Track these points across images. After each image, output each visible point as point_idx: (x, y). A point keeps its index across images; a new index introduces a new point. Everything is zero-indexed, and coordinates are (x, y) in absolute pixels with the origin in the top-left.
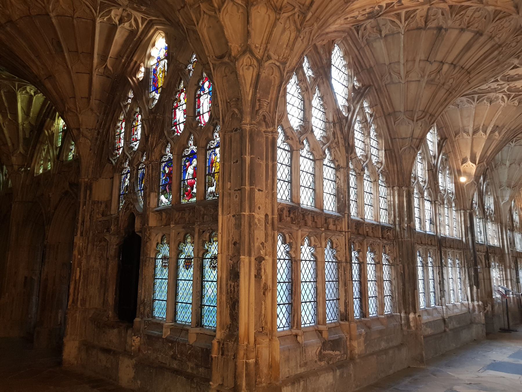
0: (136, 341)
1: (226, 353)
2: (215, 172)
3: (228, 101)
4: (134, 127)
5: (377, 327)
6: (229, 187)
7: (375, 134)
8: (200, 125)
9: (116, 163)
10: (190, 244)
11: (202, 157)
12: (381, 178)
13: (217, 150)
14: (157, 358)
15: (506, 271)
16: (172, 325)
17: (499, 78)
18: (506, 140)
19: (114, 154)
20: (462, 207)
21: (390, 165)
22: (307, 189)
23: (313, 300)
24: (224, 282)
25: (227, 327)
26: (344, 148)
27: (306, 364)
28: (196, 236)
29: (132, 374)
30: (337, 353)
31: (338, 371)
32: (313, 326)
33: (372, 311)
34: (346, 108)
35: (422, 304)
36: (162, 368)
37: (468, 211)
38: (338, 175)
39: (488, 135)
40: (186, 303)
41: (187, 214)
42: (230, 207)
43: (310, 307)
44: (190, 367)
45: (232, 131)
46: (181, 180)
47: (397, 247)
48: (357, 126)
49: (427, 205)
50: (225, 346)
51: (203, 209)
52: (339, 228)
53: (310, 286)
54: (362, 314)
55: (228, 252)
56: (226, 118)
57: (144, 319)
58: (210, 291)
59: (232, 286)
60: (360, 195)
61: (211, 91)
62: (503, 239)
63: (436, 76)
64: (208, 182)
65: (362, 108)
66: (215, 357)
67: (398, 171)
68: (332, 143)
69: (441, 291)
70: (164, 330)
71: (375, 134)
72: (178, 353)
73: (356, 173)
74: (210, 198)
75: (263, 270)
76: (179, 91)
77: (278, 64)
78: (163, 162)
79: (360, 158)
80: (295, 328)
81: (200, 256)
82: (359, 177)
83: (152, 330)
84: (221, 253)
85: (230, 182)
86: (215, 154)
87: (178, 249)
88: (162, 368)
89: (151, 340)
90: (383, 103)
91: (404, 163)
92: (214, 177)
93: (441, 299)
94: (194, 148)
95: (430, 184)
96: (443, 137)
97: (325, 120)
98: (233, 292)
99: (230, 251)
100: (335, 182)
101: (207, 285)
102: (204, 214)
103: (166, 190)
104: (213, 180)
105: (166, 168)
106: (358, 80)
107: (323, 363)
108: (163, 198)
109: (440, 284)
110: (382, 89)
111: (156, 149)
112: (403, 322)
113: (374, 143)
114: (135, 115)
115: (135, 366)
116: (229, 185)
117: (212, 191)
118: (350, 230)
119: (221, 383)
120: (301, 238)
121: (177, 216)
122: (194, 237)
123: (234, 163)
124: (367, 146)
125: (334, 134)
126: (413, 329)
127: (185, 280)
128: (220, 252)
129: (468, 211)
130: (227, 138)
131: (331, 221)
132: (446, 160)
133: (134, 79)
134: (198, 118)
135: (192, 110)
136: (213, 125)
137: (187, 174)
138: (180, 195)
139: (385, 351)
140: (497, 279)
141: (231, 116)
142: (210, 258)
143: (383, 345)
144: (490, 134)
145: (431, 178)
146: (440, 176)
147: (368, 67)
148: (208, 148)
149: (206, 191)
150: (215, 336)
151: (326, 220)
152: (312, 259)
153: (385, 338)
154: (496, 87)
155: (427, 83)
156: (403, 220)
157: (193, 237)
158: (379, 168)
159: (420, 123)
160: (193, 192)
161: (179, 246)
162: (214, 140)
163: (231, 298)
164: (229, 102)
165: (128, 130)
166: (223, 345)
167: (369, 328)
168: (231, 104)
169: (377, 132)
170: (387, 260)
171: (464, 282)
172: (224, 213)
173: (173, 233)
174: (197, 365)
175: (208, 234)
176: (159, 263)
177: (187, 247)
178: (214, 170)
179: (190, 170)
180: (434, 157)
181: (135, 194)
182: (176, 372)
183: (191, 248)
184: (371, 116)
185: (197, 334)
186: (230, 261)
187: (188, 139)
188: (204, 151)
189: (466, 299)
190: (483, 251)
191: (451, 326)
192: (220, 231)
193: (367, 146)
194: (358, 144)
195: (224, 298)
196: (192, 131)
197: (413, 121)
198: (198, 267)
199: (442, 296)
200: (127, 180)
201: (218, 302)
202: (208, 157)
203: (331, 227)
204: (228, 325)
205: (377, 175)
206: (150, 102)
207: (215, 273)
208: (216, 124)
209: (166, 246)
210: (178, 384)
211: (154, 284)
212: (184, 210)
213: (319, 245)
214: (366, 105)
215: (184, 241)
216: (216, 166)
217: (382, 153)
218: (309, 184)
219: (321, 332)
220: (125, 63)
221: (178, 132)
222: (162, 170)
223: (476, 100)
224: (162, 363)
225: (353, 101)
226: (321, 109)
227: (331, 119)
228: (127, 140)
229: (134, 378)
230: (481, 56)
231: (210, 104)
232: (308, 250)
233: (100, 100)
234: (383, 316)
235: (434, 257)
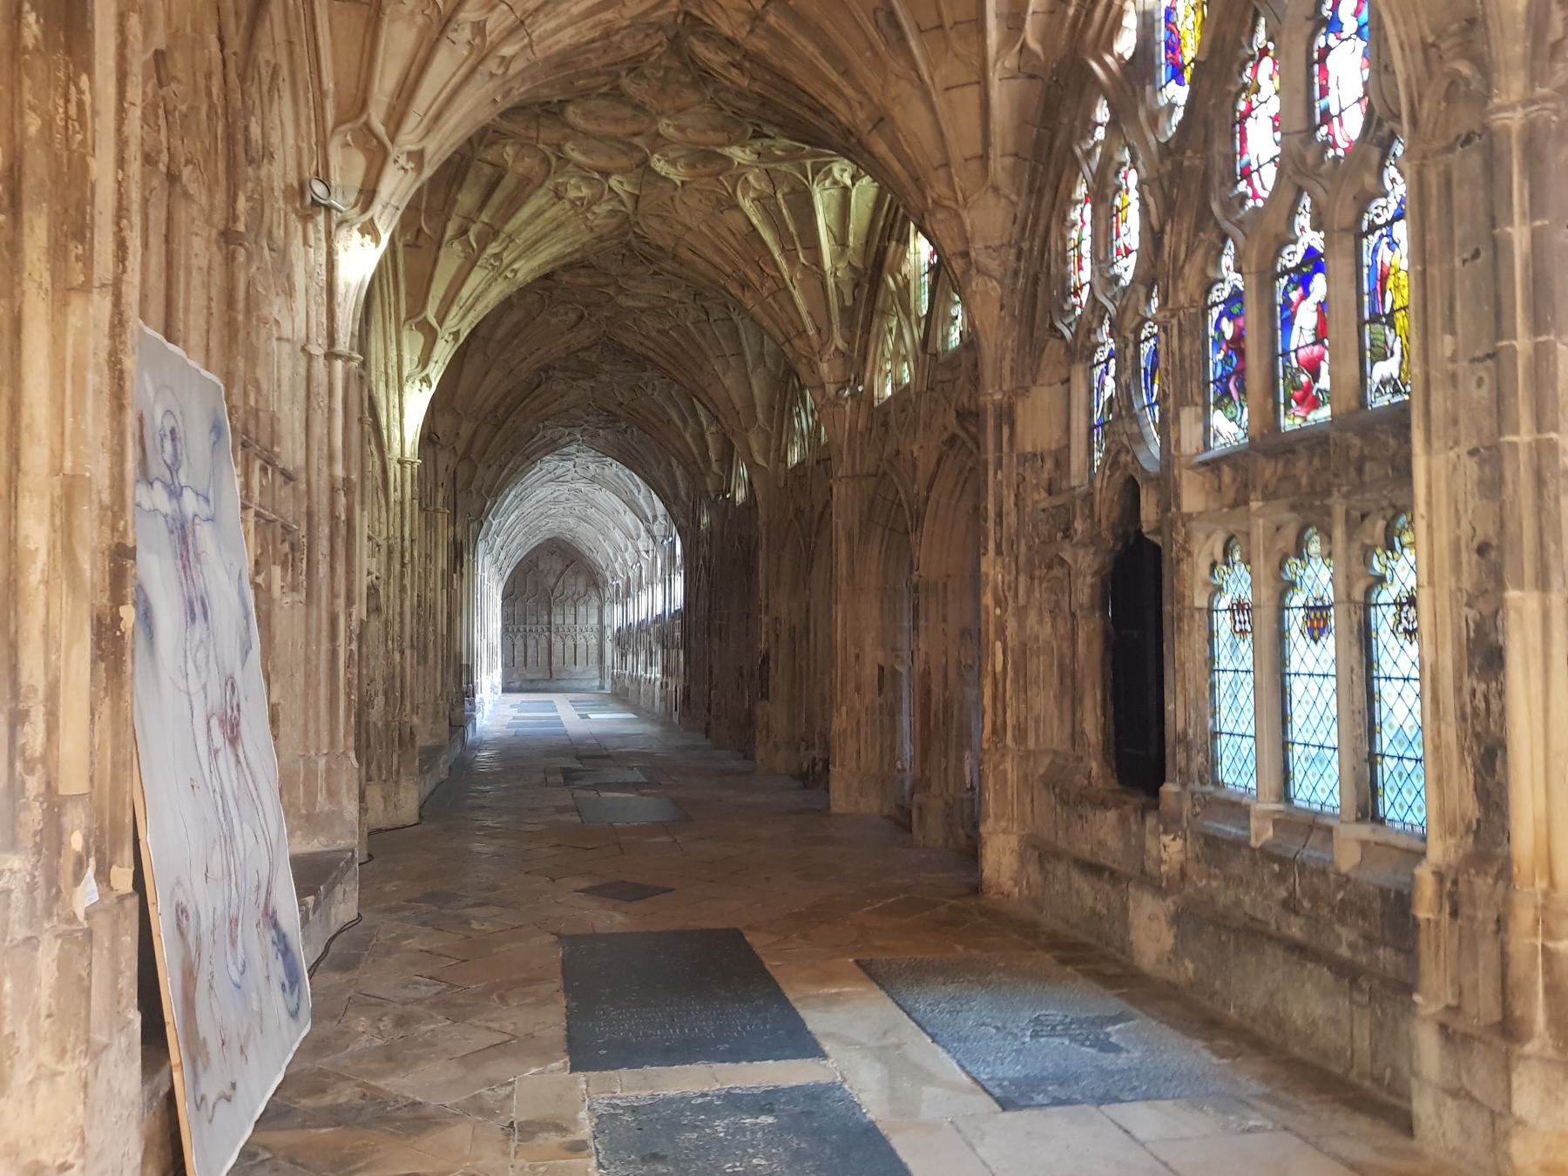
0: (1171, 850)
1: (1465, 910)
2: (1396, 306)
3: (1431, 39)
4: (1118, 211)
6: (1448, 353)
8: (1331, 153)
9: (1075, 335)
10: (1320, 560)
11: (1341, 265)
13: (1401, 230)
14: (1238, 903)
16: (1279, 812)
19: (1067, 307)
24: (1447, 682)
25: (1468, 829)
28: (1339, 532)
29: (1168, 940)
36: (1254, 934)
40: (1321, 747)
41: (1301, 464)
42: (1455, 422)
44: (1344, 940)
45: (1450, 149)
46: (1275, 354)
50: (1463, 887)
51: (1356, 442)
55: (1459, 579)
56: (1426, 105)
57: (1190, 786)
58: (1400, 711)
59: (1479, 695)
61: (1365, 24)
64: (1372, 345)
66: (1428, 920)
70: (1253, 823)
72: (1304, 894)
74: (1383, 401)
76: (1252, 57)
78: (1215, 304)
81: (1358, 595)
83: (1217, 822)
84: (1431, 583)
85: (1453, 333)
86: (1393, 245)
87: (1278, 579)
88: (1254, 934)
89: (1215, 849)
92: (1392, 326)
94: (1316, 240)
98: (1483, 713)
99: (1465, 576)
101: (1387, 690)
102: (1362, 459)
103: (1227, 393)
104: (1390, 337)
105: (1225, 321)
108: (1218, 419)
114: (1117, 173)
115: (1176, 919)
117: (1387, 375)
119: (1452, 1001)
121: (1268, 474)
122: (1330, 536)
123: (1464, 261)
127: (1311, 675)
128: (1424, 580)
130: (1433, 177)
134: (1324, 130)
135: (1299, 111)
136: (1379, 144)
137: (1296, 329)
138: (1276, 404)
141: (1442, 92)
148: (1365, 226)
149: (1363, 377)
150: (1422, 854)
157: (1327, 535)
160: (1319, 390)
161: (1281, 568)
163: (1477, 735)
164: (1433, 45)
166: (1455, 882)
168: (1443, 46)
172: (1436, 445)
173: (1259, 528)
174: (1368, 938)
175: (1381, 524)
176: (1223, 623)
177: (1309, 571)
178: (1393, 301)
179: (1306, 317)
181: (1135, 418)
182: (1298, 950)
183: (1325, 574)
185: (1364, 844)
186: (1466, 610)
187: (1293, 212)
188: (1349, 243)
192: (1421, 507)
195: (1450, 734)
196: (1304, 182)
198: (1351, 632)
201: (1429, 746)
202: (1367, 260)
204: (1470, 823)
206: (1162, 119)
207: (1413, 650)
208: (1393, 136)
209: (1241, 570)
210: (1308, 986)
211: (1212, 687)
212: (1293, 452)
215: (1300, 551)
216: (1397, 287)
220: (1076, 17)
221: (1255, 196)
224: (1253, 919)
228: (1102, 256)
229: (1174, 951)
231: (1366, 72)
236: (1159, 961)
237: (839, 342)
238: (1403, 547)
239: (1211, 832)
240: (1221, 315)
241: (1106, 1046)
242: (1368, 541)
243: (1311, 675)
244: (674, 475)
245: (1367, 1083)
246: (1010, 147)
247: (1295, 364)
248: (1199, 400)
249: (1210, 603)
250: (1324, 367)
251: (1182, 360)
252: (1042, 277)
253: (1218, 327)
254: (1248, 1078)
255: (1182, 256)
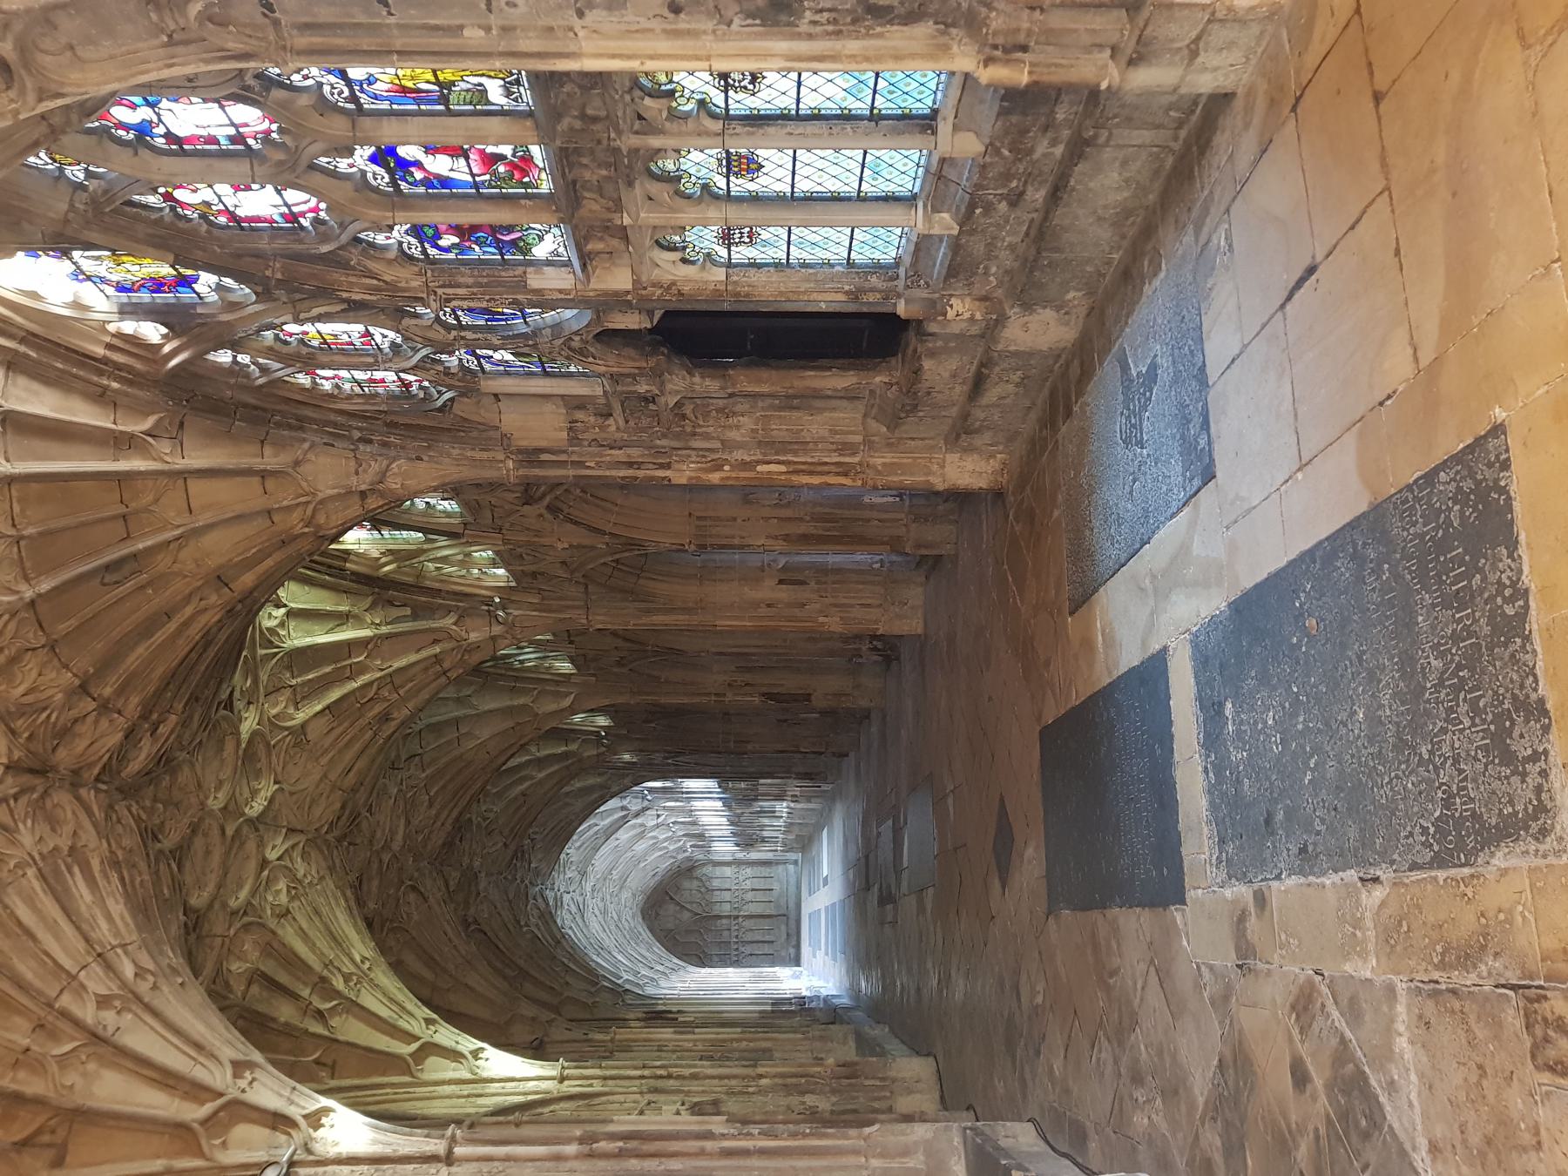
0: (961, 309)
1: (1021, 38)
2: (433, 79)
3: (165, 39)
4: (325, 342)
6: (482, 33)
8: (274, 135)
9: (450, 387)
10: (681, 160)
11: (388, 132)
13: (356, 73)
14: (1012, 248)
16: (925, 206)
19: (422, 395)
24: (803, 47)
25: (943, 33)
28: (655, 142)
29: (1048, 314)
36: (1041, 235)
40: (863, 166)
41: (587, 175)
42: (551, 29)
44: (1046, 150)
45: (276, 23)
46: (477, 194)
50: (1000, 40)
51: (565, 123)
55: (705, 32)
56: (230, 45)
58: (829, 90)
59: (817, 17)
61: (145, 99)
64: (470, 103)
66: (1030, 73)
70: (936, 231)
72: (1005, 186)
74: (526, 95)
76: (173, 209)
78: (424, 251)
81: (717, 126)
83: (934, 265)
84: (708, 58)
85: (461, 27)
86: (371, 80)
87: (700, 200)
88: (1041, 235)
89: (959, 268)
92: (453, 83)
94: (362, 154)
98: (833, 15)
99: (702, 26)
101: (810, 101)
102: (583, 116)
103: (514, 243)
104: (463, 86)
105: (441, 243)
108: (541, 251)
114: (286, 343)
115: (1028, 307)
116: (473, 35)
117: (501, 91)
121: (596, 207)
122: (659, 150)
123: (390, 14)
128: (705, 65)
130: (303, 41)
134: (251, 142)
135: (230, 165)
136: (268, 90)
137: (453, 175)
138: (527, 196)
141: (219, 28)
142: (726, 92)
148: (351, 106)
149: (502, 113)
150: (967, 76)
157: (658, 152)
160: (514, 156)
161: (689, 197)
162: (320, 85)
163: (854, 22)
164: (170, 36)
165: (337, 358)
166: (995, 47)
168: (172, 26)
172: (572, 48)
173: (648, 217)
174: (1046, 129)
175: (648, 101)
176: (742, 253)
177: (692, 171)
178: (428, 82)
179: (440, 165)
181: (536, 333)
182: (1057, 193)
183: (696, 156)
185: (956, 128)
186: (734, 27)
187: (334, 174)
188: (366, 122)
192: (634, 65)
195: (853, 46)
196: (304, 162)
198: (753, 133)
200: (497, 356)
201: (865, 65)
202: (385, 106)
204: (938, 30)
206: (232, 297)
207: (771, 77)
208: (260, 76)
209: (690, 236)
210: (1092, 185)
211: (804, 265)
212: (574, 182)
215: (673, 179)
216: (413, 78)
221: (316, 210)
222: (451, 256)
224: (1027, 234)
228: (371, 360)
229: (1058, 309)
231: (194, 100)
233: (262, 442)
236: (1067, 324)
237: (448, 621)
238: (671, 81)
239: (944, 272)
241: (1152, 375)
242: (665, 114)
243: (794, 173)
244: (580, 789)
245: (1183, 133)
246: (255, 448)
247: (487, 177)
248: (519, 271)
249: (721, 265)
250: (490, 149)
251: (480, 285)
252: (389, 419)
254: (1179, 245)
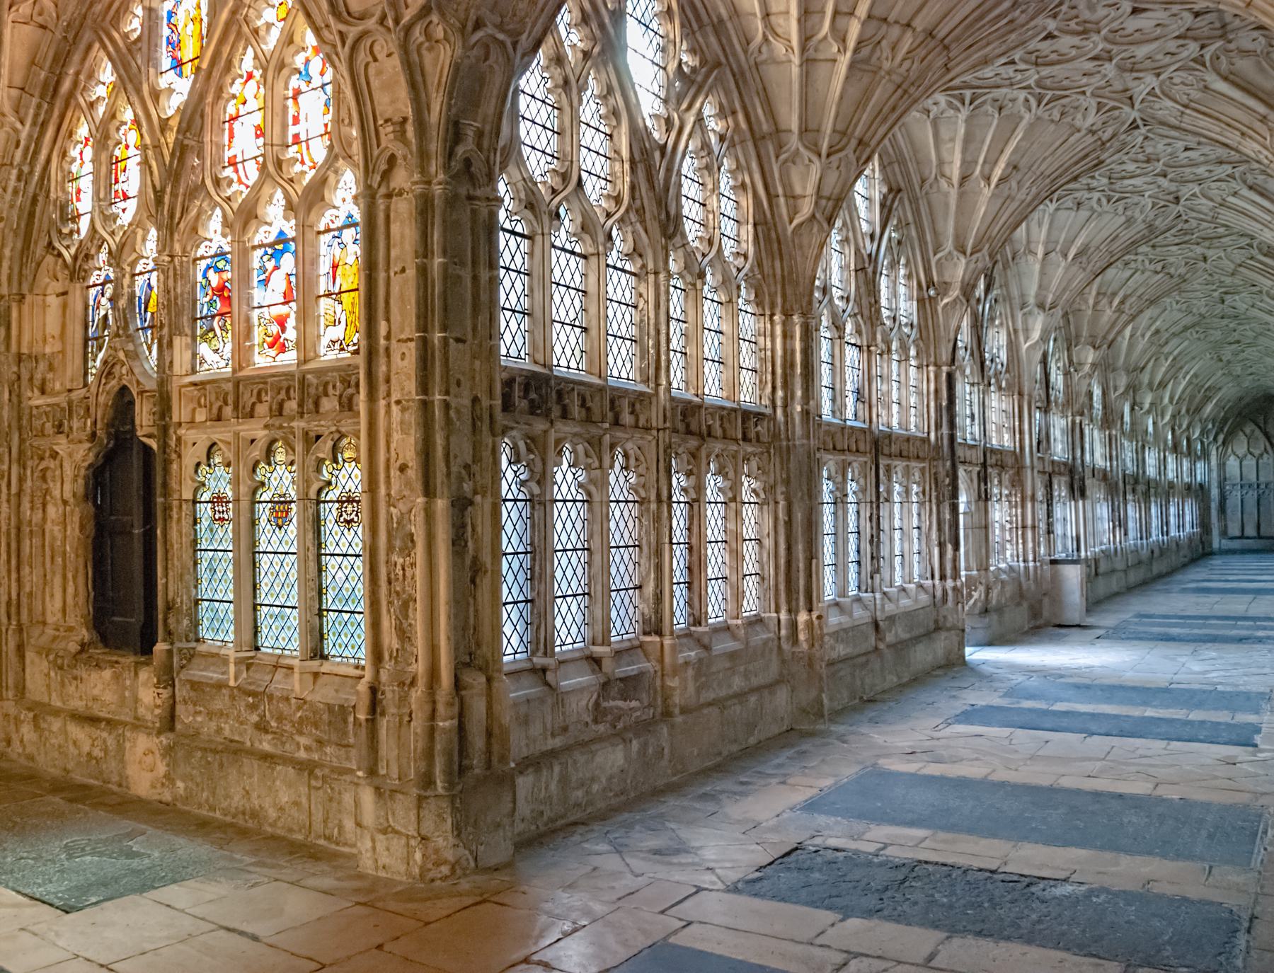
4: (117, 162)
5: (723, 645)
7: (732, 182)
9: (75, 258)
12: (743, 292)
15: (1023, 507)
17: (1017, 58)
18: (1033, 200)
20: (932, 359)
21: (765, 262)
22: (568, 328)
23: (580, 591)
26: (656, 225)
27: (565, 729)
30: (634, 704)
31: (634, 742)
32: (581, 649)
33: (715, 612)
34: (663, 122)
35: (829, 591)
37: (945, 369)
38: (642, 289)
39: (993, 186)
43: (574, 608)
47: (778, 459)
48: (688, 166)
49: (851, 354)
52: (642, 422)
53: (574, 560)
54: (691, 619)
57: (178, 645)
59: (399, 567)
60: (694, 335)
62: (1021, 432)
63: (873, 51)
65: (700, 119)
67: (783, 276)
68: (627, 211)
69: (872, 558)
71: (732, 182)
73: (685, 283)
75: (469, 528)
76: (241, 76)
77: (501, 36)
78: (203, 258)
79: (696, 244)
80: (540, 654)
81: (313, 495)
82: (693, 291)
88: (235, 751)
90: (750, 109)
91: (799, 259)
93: (872, 578)
95: (860, 306)
96: (894, 186)
97: (612, 155)
100: (636, 307)
103: (212, 330)
105: (211, 272)
106: (692, 51)
107: (601, 728)
108: (204, 349)
109: (871, 542)
110: (748, 75)
111: (182, 225)
112: (783, 632)
113: (728, 207)
114: (118, 129)
118: (668, 425)
120: (556, 447)
124: (711, 216)
125: (633, 188)
126: (805, 646)
127: (275, 553)
129: (945, 369)
131: (625, 405)
132: (899, 243)
133: (116, 35)
139: (741, 696)
140: (1003, 528)
142: (338, 501)
143: (738, 683)
144: (997, 186)
145: (863, 290)
146: (884, 282)
147: (715, 20)
151: (612, 402)
152: (579, 497)
153: (742, 669)
154: (1012, 74)
155: (852, 66)
156: (793, 398)
157: (290, 447)
158: (739, 270)
159: (834, 158)
161: (254, 471)
165: (104, 169)
167: (707, 648)
169: (735, 179)
170: (754, 491)
171: (928, 537)
174: (320, 742)
175: (330, 443)
176: (205, 511)
177: (275, 474)
180: (872, 237)
181: (130, 338)
183: (287, 478)
184: (722, 138)
189: (929, 575)
190: (974, 461)
191: (890, 638)
193: (711, 216)
194: (690, 210)
197: (820, 155)
199: (877, 570)
200: (104, 301)
203: (627, 418)
205: (734, 287)
206: (163, 99)
211: (196, 564)
213: (596, 464)
214: (708, 110)
217: (748, 232)
218: (572, 315)
219: (596, 661)
222: (199, 278)
223: (967, 102)
225: (679, 103)
226: (602, 128)
227: (625, 153)
228: (102, 195)
230: (973, 11)
232: (569, 477)
233: (23, 89)
234: (739, 622)
235: (862, 481)
236: (153, 787)
238: (344, 461)
239: (196, 679)
240: (209, 267)
241: (131, 855)
242: (321, 455)
243: (275, 553)
245: (322, 842)
248: (188, 331)
249: (195, 496)
251: (176, 299)
252: (40, 199)
253: (205, 276)
254: (242, 855)
255: (178, 215)
